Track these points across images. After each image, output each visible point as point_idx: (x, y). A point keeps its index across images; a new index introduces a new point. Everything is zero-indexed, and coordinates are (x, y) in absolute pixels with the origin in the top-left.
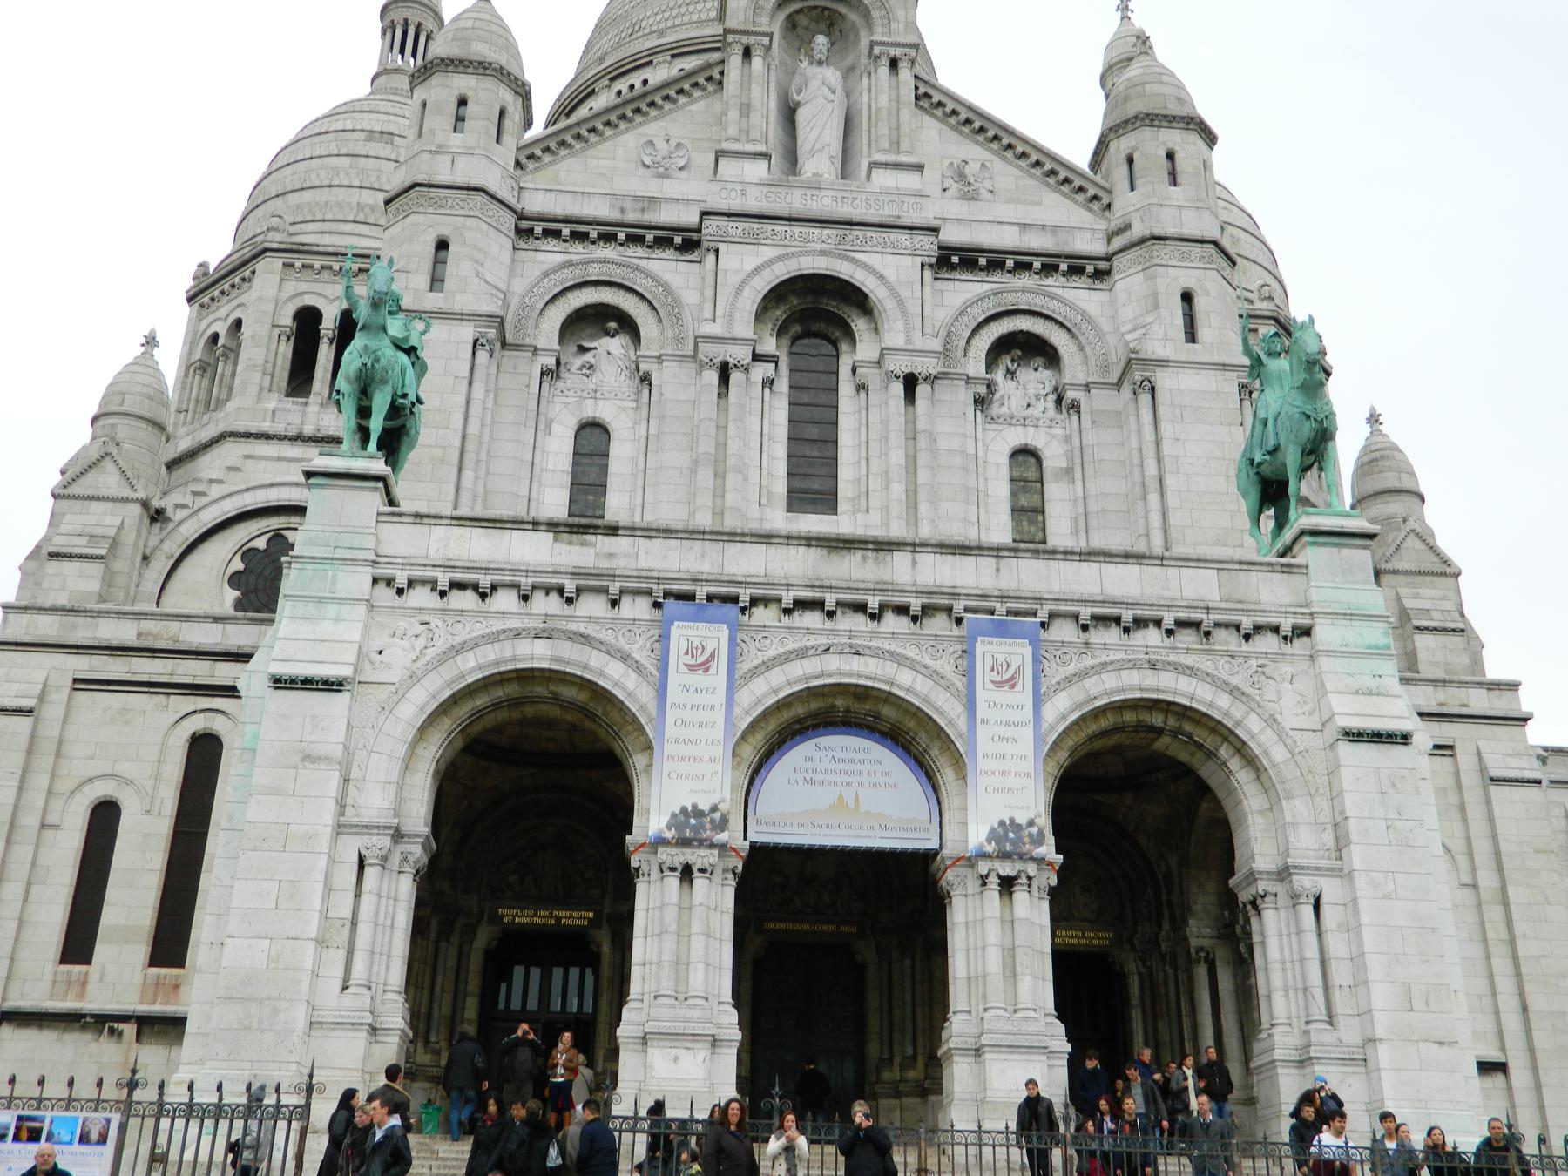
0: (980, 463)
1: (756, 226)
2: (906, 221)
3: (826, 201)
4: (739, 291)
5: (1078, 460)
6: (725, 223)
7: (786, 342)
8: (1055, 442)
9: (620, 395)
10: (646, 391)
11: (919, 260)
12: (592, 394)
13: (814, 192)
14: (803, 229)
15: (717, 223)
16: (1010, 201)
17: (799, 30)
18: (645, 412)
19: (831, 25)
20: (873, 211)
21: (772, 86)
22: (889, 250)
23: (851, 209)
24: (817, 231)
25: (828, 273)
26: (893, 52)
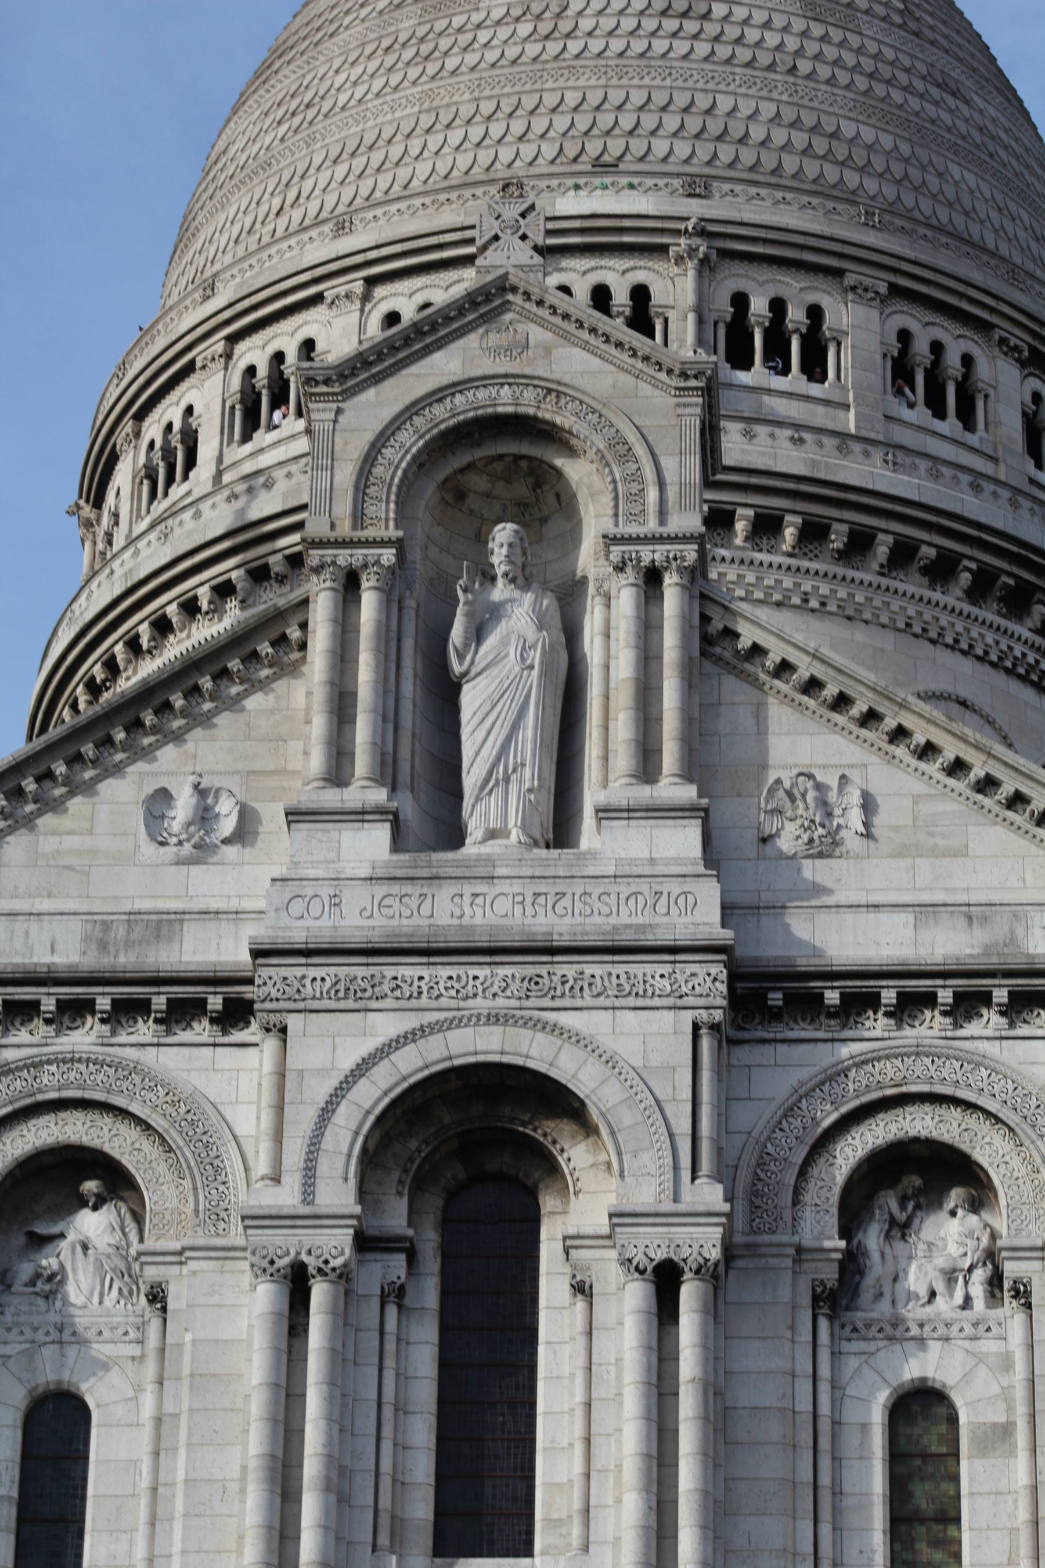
0: (825, 1426)
1: (361, 972)
2: (663, 937)
3: (503, 906)
5: (1021, 1409)
6: (299, 972)
7: (433, 1202)
8: (983, 1371)
9: (106, 1334)
10: (155, 1324)
11: (687, 1018)
12: (54, 1335)
13: (480, 888)
14: (453, 971)
15: (284, 972)
16: (900, 853)
17: (472, 501)
18: (151, 1368)
19: (538, 485)
20: (596, 919)
22: (631, 1001)
24: (483, 972)
25: (505, 1059)
26: (649, 554)
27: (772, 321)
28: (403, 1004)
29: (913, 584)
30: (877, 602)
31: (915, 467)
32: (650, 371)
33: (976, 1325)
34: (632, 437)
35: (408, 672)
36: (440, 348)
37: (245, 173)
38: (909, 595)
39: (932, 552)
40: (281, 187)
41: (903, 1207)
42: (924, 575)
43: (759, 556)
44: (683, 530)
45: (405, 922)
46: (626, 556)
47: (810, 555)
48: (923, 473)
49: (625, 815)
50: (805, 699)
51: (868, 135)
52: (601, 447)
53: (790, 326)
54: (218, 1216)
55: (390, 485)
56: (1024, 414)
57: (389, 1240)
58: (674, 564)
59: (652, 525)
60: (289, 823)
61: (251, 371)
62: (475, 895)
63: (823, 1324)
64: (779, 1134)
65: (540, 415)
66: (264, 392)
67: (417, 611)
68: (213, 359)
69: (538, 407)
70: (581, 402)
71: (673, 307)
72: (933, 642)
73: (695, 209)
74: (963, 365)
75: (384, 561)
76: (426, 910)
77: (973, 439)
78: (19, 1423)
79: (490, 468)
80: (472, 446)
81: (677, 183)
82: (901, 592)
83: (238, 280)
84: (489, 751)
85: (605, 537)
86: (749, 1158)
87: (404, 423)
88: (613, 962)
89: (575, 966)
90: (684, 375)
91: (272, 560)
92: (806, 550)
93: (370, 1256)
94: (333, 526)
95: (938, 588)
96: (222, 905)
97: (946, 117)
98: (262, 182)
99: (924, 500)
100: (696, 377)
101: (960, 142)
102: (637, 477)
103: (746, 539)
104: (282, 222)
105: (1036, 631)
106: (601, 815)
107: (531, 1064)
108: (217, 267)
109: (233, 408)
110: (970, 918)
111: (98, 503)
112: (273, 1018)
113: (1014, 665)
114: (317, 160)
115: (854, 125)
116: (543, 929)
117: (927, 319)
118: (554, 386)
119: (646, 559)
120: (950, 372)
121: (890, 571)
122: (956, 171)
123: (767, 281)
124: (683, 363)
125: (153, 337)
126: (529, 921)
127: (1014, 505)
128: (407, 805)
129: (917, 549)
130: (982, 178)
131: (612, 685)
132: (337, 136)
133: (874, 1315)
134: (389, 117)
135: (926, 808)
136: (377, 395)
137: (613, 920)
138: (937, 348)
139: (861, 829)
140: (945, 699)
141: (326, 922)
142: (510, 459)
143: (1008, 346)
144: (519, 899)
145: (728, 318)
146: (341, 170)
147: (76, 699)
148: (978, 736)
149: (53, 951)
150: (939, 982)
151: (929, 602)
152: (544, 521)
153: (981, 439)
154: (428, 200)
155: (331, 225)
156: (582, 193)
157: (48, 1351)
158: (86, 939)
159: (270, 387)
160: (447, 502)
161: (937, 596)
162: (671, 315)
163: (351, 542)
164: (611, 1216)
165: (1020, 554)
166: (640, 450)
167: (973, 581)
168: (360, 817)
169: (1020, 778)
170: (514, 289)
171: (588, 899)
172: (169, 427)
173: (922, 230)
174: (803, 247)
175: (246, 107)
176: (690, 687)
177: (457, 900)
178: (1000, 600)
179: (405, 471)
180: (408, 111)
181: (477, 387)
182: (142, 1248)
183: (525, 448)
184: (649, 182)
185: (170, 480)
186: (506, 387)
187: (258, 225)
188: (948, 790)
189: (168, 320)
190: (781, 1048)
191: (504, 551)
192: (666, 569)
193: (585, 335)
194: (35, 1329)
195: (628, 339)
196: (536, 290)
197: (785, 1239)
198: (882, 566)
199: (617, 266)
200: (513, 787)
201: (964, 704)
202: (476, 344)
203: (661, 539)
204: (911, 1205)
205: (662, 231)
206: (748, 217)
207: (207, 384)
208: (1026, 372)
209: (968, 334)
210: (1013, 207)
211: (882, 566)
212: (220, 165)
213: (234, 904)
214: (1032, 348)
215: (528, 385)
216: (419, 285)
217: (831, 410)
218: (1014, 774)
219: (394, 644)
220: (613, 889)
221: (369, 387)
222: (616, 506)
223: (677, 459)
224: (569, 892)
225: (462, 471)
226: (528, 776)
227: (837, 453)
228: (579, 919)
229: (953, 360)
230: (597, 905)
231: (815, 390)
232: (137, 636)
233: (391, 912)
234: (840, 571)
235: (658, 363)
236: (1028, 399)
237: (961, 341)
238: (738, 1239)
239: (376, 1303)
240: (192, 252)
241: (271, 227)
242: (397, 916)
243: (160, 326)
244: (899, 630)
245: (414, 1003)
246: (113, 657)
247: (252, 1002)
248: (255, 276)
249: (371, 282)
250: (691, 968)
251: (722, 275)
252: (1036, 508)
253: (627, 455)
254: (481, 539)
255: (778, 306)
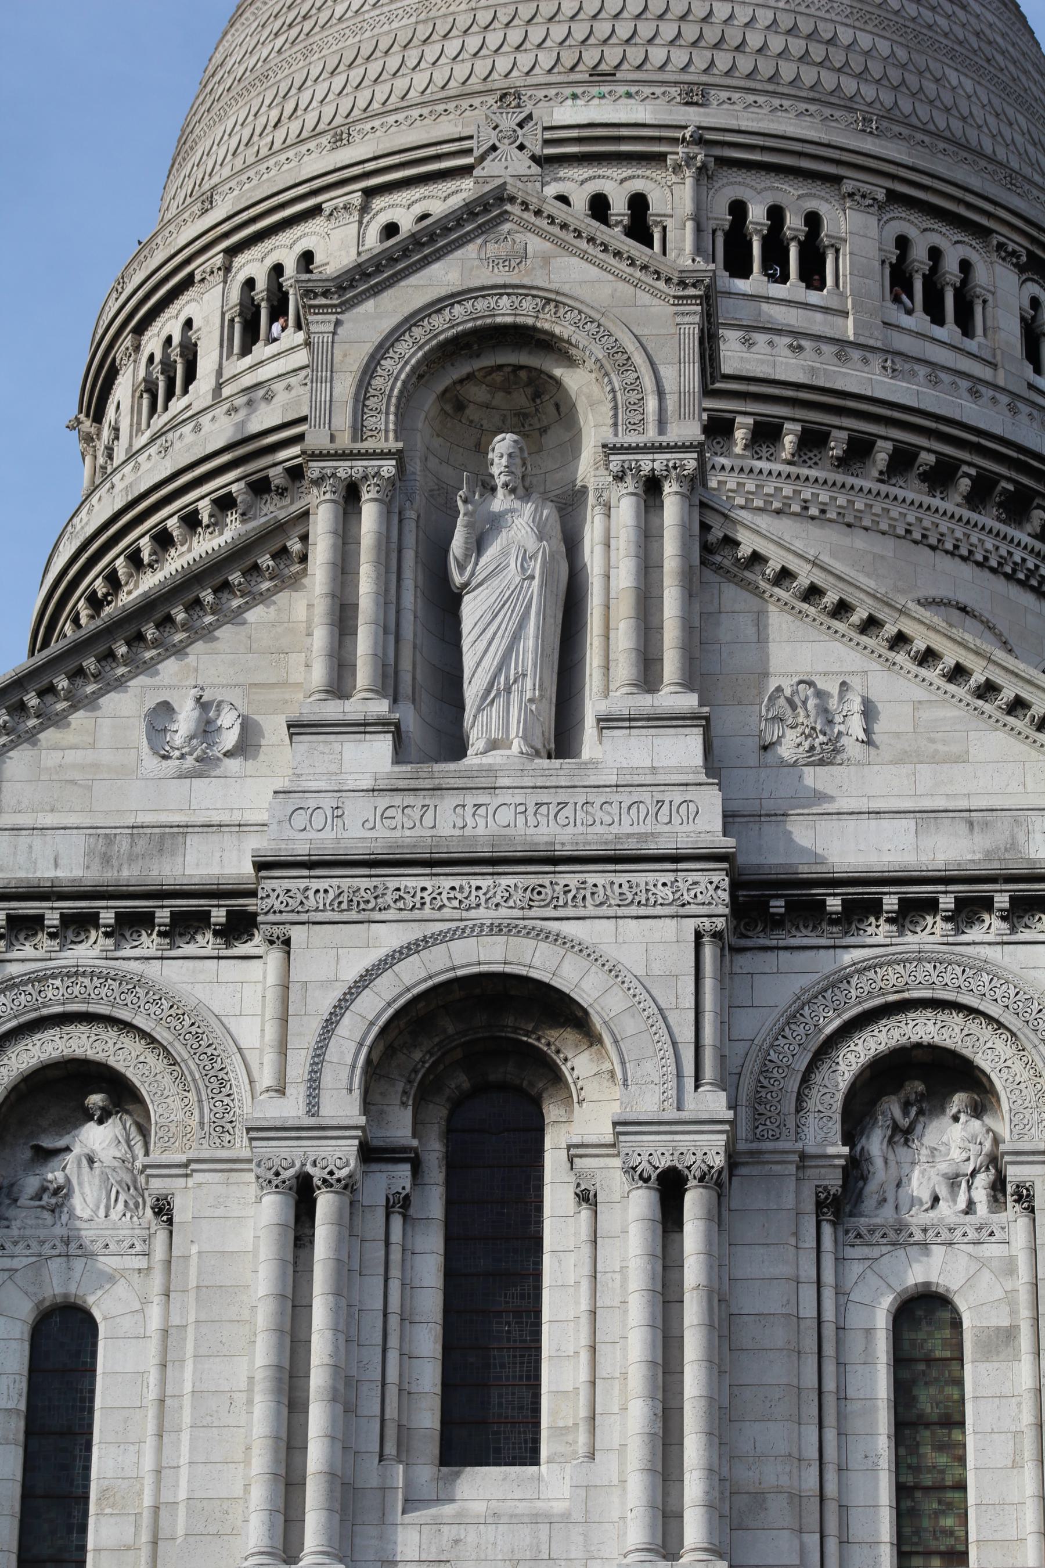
0: (829, 1331)
1: (364, 883)
2: (665, 845)
3: (505, 816)
4: (330, 1024)
5: (1025, 1313)
6: (302, 884)
7: (438, 1113)
8: (986, 1276)
10: (161, 1236)
11: (690, 925)
12: (61, 1249)
14: (456, 882)
15: (287, 884)
17: (471, 412)
19: (537, 395)
20: (598, 829)
21: (409, 556)
22: (634, 910)
23: (554, 828)
24: (485, 883)
25: (508, 969)
26: (648, 464)
27: (770, 229)
28: (406, 915)
29: (912, 491)
30: (877, 509)
31: (914, 374)
32: (649, 280)
33: (979, 1229)
34: (631, 346)
35: (409, 583)
36: (438, 259)
37: (242, 85)
38: (908, 502)
39: (931, 459)
40: (278, 100)
41: (906, 1113)
42: (923, 481)
43: (759, 464)
44: (682, 439)
45: (408, 833)
46: (626, 465)
47: (810, 463)
48: (922, 379)
49: (626, 724)
50: (805, 606)
51: (865, 41)
52: (600, 356)
53: (788, 233)
54: (222, 1129)
55: (390, 397)
56: (1023, 319)
57: (394, 1150)
58: (673, 473)
59: (651, 434)
60: (291, 735)
61: (250, 283)
62: (478, 806)
63: (827, 1230)
64: (782, 1041)
65: (539, 325)
66: (263, 304)
67: (417, 522)
68: (212, 272)
69: (537, 317)
70: (580, 312)
71: (671, 216)
72: (933, 548)
73: (693, 117)
74: (961, 271)
75: (384, 472)
76: (428, 820)
77: (971, 345)
78: (27, 1336)
79: (489, 378)
80: (471, 357)
81: (674, 91)
82: (900, 499)
83: (236, 193)
84: (490, 662)
85: (604, 446)
86: (752, 1066)
87: (403, 334)
88: (615, 871)
89: (577, 875)
90: (683, 284)
91: (272, 472)
92: (805, 458)
93: (374, 1167)
94: (332, 439)
95: (938, 494)
96: (225, 818)
97: (943, 22)
98: (259, 94)
99: (922, 406)
100: (694, 285)
101: (956, 47)
102: (636, 386)
103: (746, 447)
104: (280, 135)
105: (1035, 537)
106: (602, 724)
107: (534, 974)
108: (216, 179)
109: (232, 320)
110: (971, 824)
111: (98, 418)
112: (277, 931)
113: (1014, 571)
114: (314, 73)
115: (851, 31)
116: (546, 839)
117: (925, 225)
118: (552, 296)
119: (646, 467)
120: (948, 277)
121: (889, 478)
122: (953, 77)
123: (766, 189)
124: (681, 272)
125: (152, 251)
126: (531, 831)
127: (1013, 410)
128: (408, 716)
129: (916, 455)
130: (979, 83)
131: (612, 595)
132: (334, 48)
133: (878, 1221)
134: (386, 27)
135: (927, 714)
136: (376, 307)
137: (615, 829)
138: (935, 254)
139: (862, 736)
140: (945, 604)
141: (328, 834)
142: (509, 369)
143: (1005, 251)
144: (521, 809)
145: (727, 227)
146: (338, 82)
147: (78, 614)
148: (978, 642)
149: (56, 866)
150: (941, 888)
151: (929, 508)
152: (543, 431)
153: (979, 344)
154: (425, 111)
155: (328, 136)
156: (579, 102)
157: (55, 1265)
158: (90, 853)
159: (269, 300)
160: (446, 413)
161: (936, 502)
162: (669, 223)
163: (351, 454)
164: (615, 1124)
165: (1019, 459)
166: (639, 359)
167: (973, 487)
168: (362, 729)
169: (1020, 684)
170: (512, 199)
171: (590, 809)
172: (169, 340)
173: (919, 136)
174: (800, 154)
175: (242, 20)
176: (691, 596)
177: (459, 810)
178: (1000, 505)
179: (404, 382)
180: (405, 21)
181: (476, 298)
182: (148, 1160)
183: (524, 358)
184: (647, 90)
185: (170, 394)
186: (505, 297)
187: (255, 138)
188: (948, 695)
189: (166, 233)
190: (784, 955)
191: (504, 461)
192: (666, 477)
193: (583, 244)
194: (42, 1243)
195: (627, 249)
196: (535, 200)
197: (788, 1145)
198: (881, 473)
199: (615, 175)
200: (515, 698)
201: (963, 609)
202: (474, 255)
203: (661, 448)
204: (914, 1111)
205: (659, 139)
206: (745, 124)
207: (206, 297)
208: (1024, 277)
209: (966, 239)
210: (1010, 112)
211: (881, 473)
212: (217, 78)
213: (236, 817)
214: (1030, 253)
215: (527, 295)
216: (418, 196)
217: (830, 317)
218: (1014, 680)
219: (394, 556)
220: (616, 798)
221: (368, 298)
222: (616, 416)
223: (676, 367)
224: (572, 801)
225: (461, 381)
226: (529, 687)
227: (836, 360)
228: (581, 829)
229: (951, 265)
230: (599, 815)
231: (814, 297)
232: (138, 550)
233: (393, 823)
234: (840, 478)
235: (656, 272)
236: (1026, 304)
237: (959, 246)
238: (742, 1146)
239: (381, 1213)
240: (190, 165)
241: (269, 139)
242: (399, 827)
243: (159, 240)
244: (899, 537)
245: (417, 914)
246: (115, 571)
247: (255, 915)
248: (254, 188)
249: (370, 193)
250: (693, 877)
251: (720, 183)
252: (1035, 413)
253: (627, 364)
254: (481, 449)
255: (776, 214)
